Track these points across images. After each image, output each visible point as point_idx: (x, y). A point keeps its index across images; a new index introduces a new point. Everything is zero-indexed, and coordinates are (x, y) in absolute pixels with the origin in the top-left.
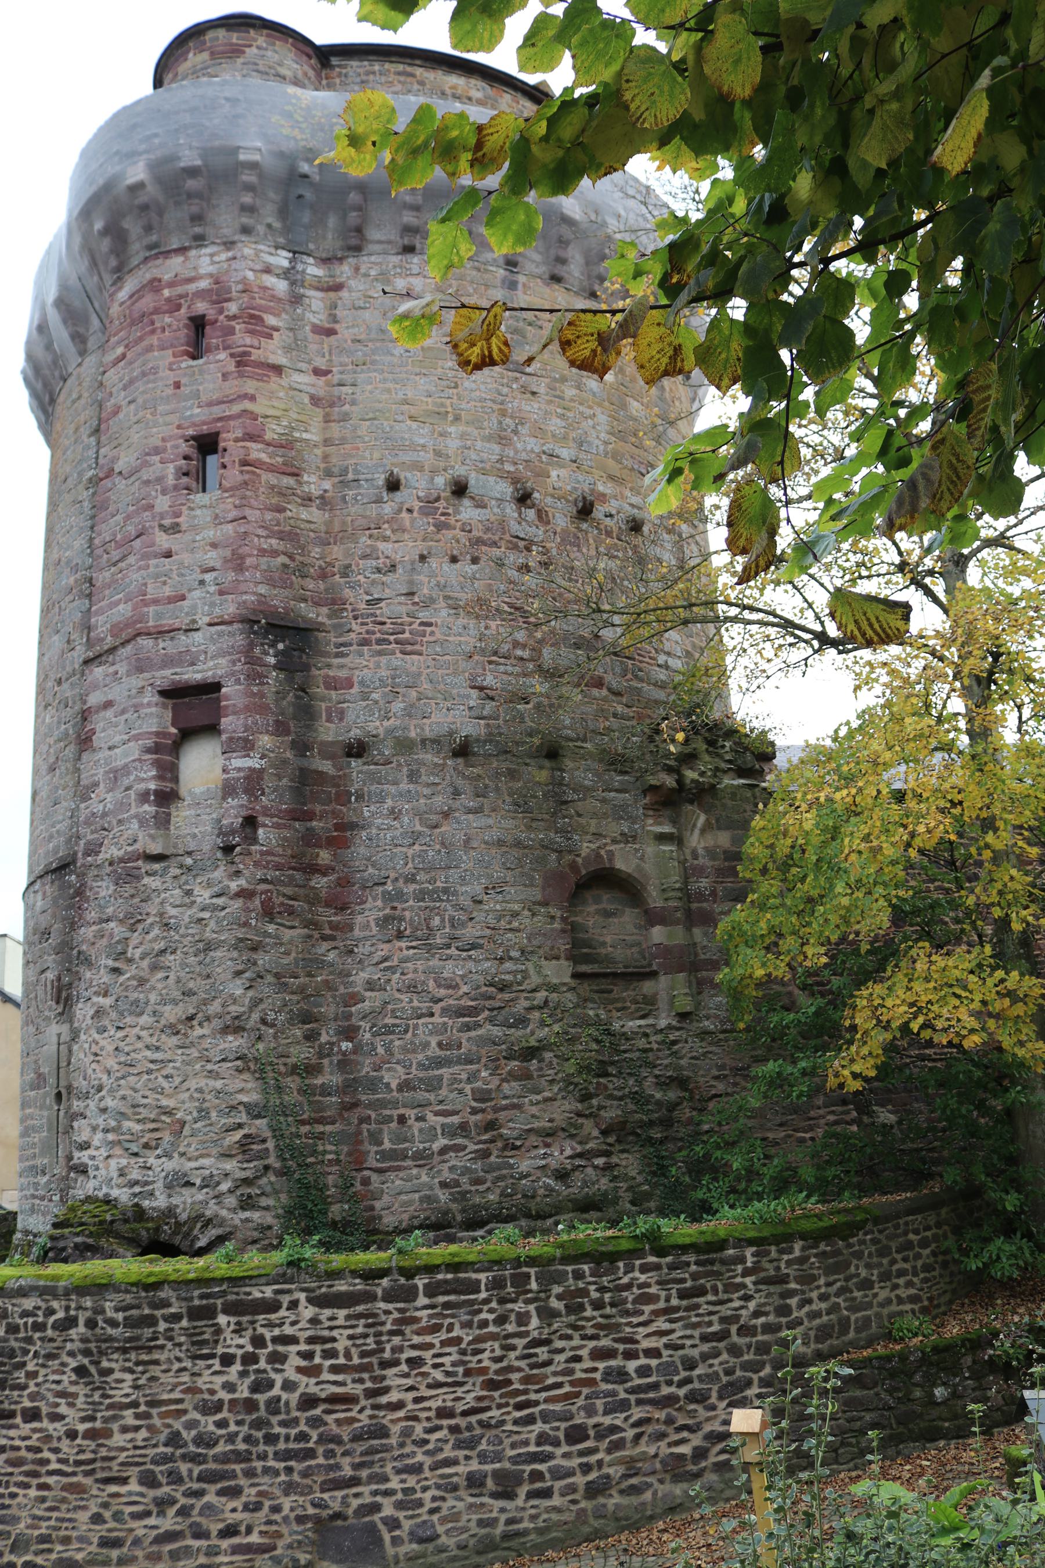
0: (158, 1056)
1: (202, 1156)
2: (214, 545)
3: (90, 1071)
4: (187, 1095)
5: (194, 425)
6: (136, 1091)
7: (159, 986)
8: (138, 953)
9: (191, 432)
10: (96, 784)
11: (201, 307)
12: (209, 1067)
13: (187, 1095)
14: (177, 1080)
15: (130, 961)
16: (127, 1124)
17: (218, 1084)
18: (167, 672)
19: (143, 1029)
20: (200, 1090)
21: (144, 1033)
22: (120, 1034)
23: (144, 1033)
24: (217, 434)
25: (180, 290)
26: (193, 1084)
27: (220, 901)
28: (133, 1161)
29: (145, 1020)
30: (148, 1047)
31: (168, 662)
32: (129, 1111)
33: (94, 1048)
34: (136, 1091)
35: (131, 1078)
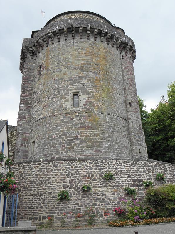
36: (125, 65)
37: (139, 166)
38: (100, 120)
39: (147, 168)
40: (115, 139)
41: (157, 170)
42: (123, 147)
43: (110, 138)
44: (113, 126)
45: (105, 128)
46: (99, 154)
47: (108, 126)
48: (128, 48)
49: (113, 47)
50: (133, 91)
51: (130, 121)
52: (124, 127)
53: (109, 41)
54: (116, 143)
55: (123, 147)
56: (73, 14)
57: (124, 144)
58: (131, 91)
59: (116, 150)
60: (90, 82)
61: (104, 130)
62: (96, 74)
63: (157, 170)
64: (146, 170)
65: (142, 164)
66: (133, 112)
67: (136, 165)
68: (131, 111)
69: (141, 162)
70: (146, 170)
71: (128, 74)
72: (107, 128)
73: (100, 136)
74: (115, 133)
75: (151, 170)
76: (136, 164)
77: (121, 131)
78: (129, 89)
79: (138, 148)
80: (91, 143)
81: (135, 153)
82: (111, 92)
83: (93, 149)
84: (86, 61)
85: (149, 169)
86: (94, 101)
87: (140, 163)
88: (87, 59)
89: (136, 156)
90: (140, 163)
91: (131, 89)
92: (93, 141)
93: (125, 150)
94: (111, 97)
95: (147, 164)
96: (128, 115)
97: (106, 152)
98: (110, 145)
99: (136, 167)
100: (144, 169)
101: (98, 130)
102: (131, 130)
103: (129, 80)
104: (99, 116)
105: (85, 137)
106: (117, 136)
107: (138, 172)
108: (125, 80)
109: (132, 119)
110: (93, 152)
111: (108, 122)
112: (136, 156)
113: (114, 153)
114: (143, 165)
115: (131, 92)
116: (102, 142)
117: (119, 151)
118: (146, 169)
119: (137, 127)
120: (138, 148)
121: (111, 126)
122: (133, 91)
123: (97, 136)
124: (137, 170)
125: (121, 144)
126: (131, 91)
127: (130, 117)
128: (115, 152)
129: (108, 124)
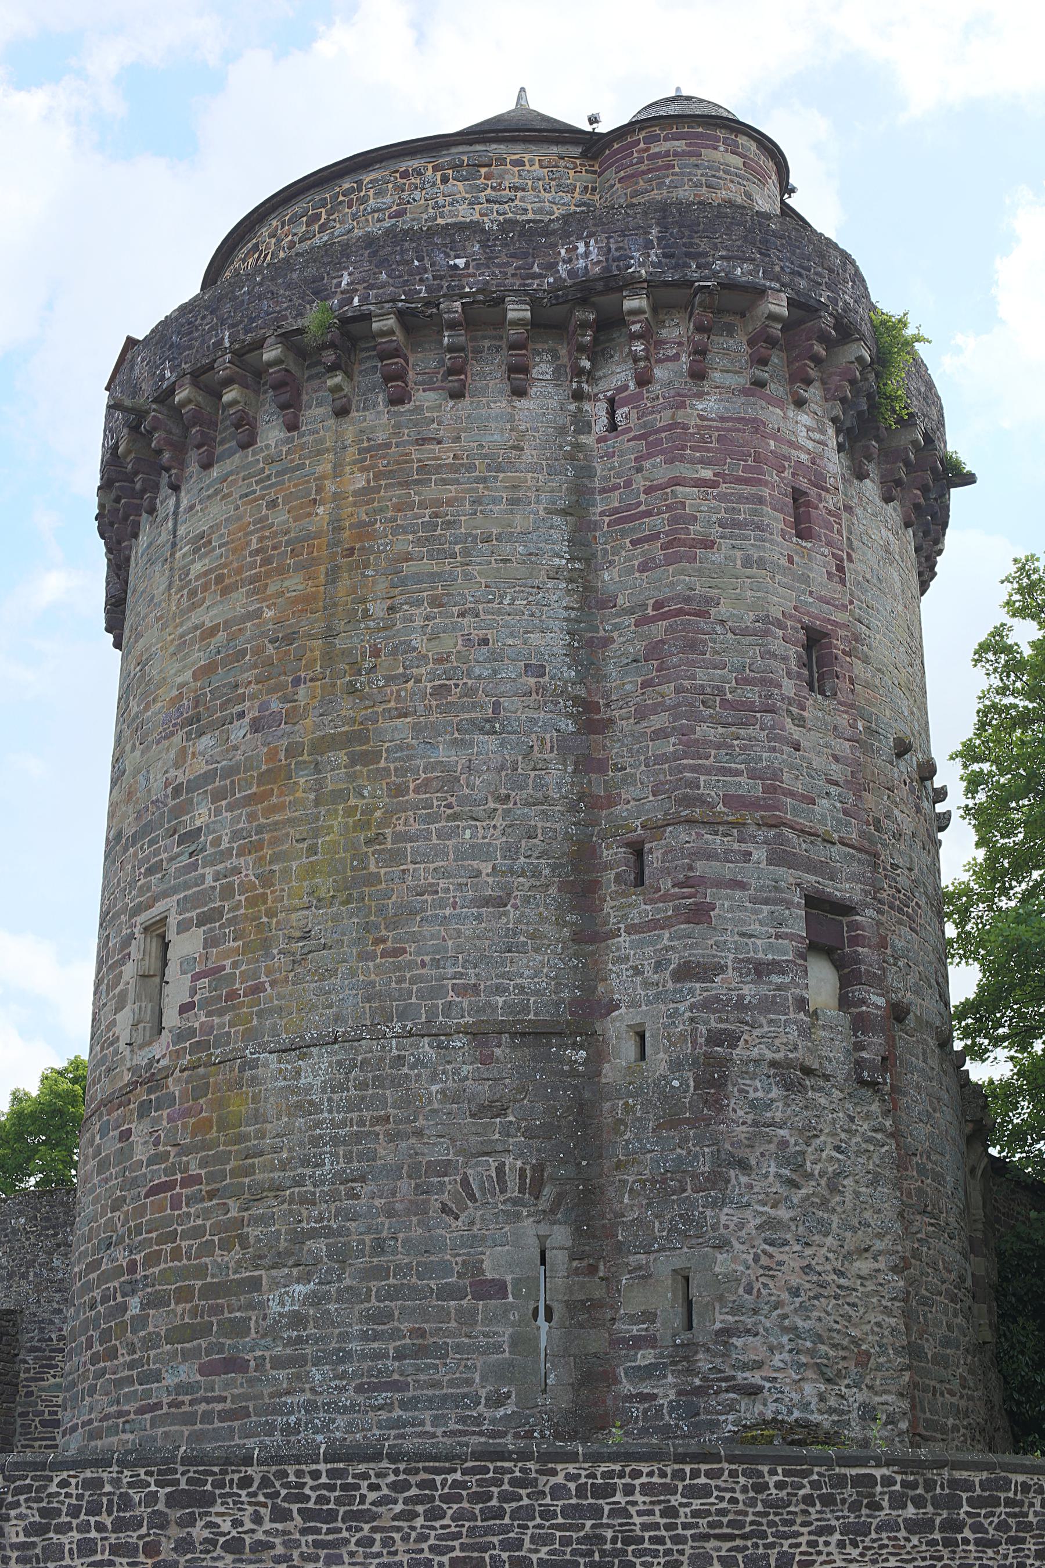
0: (842, 1281)
1: (885, 1392)
2: (836, 758)
3: (757, 1286)
4: (868, 1327)
5: (808, 614)
6: (829, 1314)
7: (839, 1209)
8: (817, 1168)
9: (806, 619)
10: (722, 969)
11: (804, 484)
12: (884, 1302)
13: (868, 1327)
14: (862, 1310)
15: (809, 1176)
16: (823, 1348)
17: (893, 1321)
18: (813, 878)
19: (829, 1251)
20: (878, 1324)
21: (831, 1255)
22: (808, 1252)
23: (831, 1255)
24: (826, 635)
25: (785, 449)
26: (873, 1317)
27: (879, 1136)
28: (829, 1387)
29: (829, 1241)
30: (835, 1271)
31: (811, 866)
32: (825, 1335)
33: (764, 1261)
34: (829, 1314)
35: (822, 1300)
36: (628, 484)
37: (44, 1512)
38: (257, 1110)
39: (108, 1522)
40: (367, 1239)
41: (210, 1525)
42: (447, 1293)
43: (318, 1246)
44: (358, 1137)
45: (284, 1166)
46: (227, 1385)
47: (315, 1141)
48: (633, 312)
49: (457, 395)
50: (676, 718)
51: (616, 1028)
52: (495, 1108)
53: (401, 376)
54: (379, 1272)
55: (447, 1293)
56: (245, 250)
57: (473, 1268)
58: (659, 721)
59: (364, 1337)
60: (230, 808)
61: (277, 1188)
62: (276, 719)
63: (210, 1525)
64: (93, 1534)
65: (68, 1495)
66: (654, 925)
67: (17, 1504)
68: (631, 929)
69: (65, 1475)
70: (93, 1534)
71: (643, 568)
72: (305, 1162)
73: (243, 1240)
74: (365, 1190)
75: (144, 1530)
76: (22, 1498)
77: (441, 1152)
78: (641, 715)
79: (664, 1265)
80: (188, 1306)
81: (633, 1319)
82: (379, 839)
83: (196, 1353)
84: (222, 635)
85: (120, 1526)
86: (235, 965)
87: (53, 1488)
88: (227, 624)
89: (640, 1342)
90: (53, 1488)
91: (655, 709)
92: (209, 1291)
93: (467, 1317)
94: (373, 879)
95: (108, 1488)
96: (589, 975)
97: (278, 1363)
98: (315, 1299)
99: (20, 1517)
100: (84, 1528)
101: (236, 1192)
102: (614, 1107)
103: (654, 620)
104: (254, 1081)
105: (163, 1266)
106: (390, 1212)
107: (30, 1553)
108: (607, 642)
109: (633, 1004)
110: (199, 1378)
111: (315, 1107)
112: (640, 1342)
113: (341, 1361)
114: (80, 1497)
115: (660, 734)
116: (255, 1284)
117: (396, 1334)
118: (100, 1527)
119: (676, 1065)
120: (664, 1265)
121: (336, 1141)
122: (676, 718)
123: (226, 1246)
124: (22, 1538)
125: (426, 1271)
126: (659, 721)
127: (618, 982)
128: (348, 1356)
129: (318, 1124)
